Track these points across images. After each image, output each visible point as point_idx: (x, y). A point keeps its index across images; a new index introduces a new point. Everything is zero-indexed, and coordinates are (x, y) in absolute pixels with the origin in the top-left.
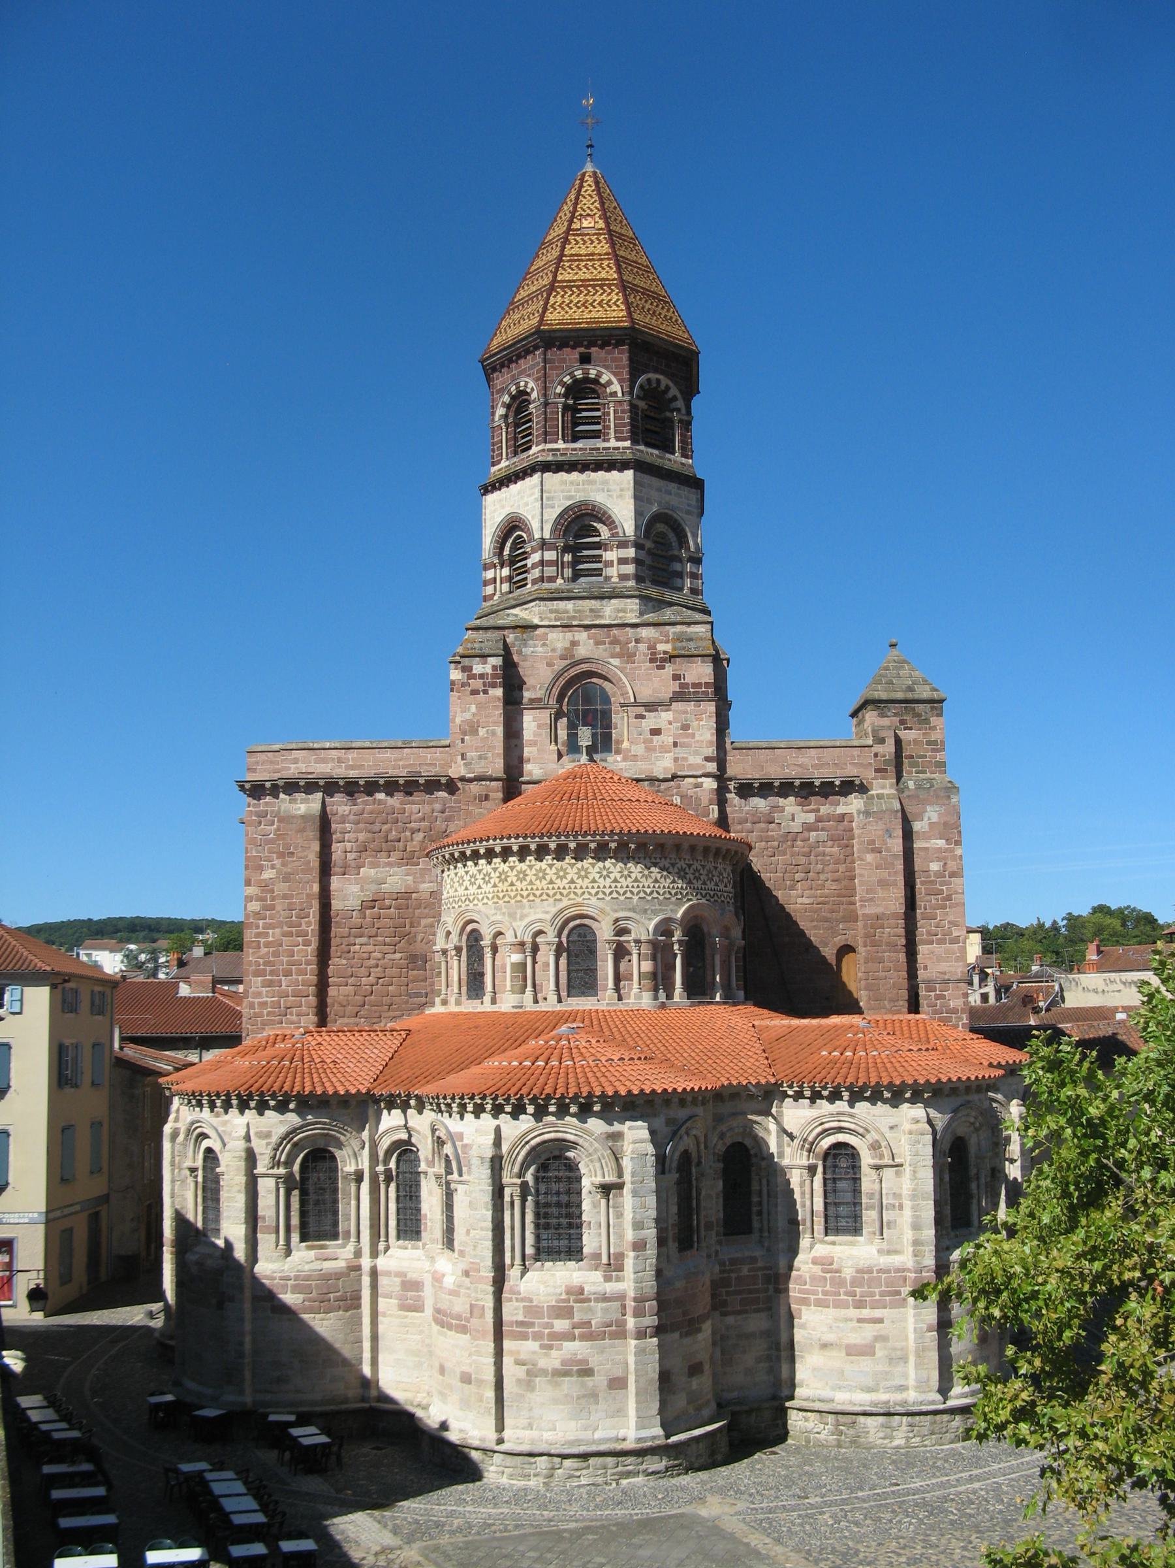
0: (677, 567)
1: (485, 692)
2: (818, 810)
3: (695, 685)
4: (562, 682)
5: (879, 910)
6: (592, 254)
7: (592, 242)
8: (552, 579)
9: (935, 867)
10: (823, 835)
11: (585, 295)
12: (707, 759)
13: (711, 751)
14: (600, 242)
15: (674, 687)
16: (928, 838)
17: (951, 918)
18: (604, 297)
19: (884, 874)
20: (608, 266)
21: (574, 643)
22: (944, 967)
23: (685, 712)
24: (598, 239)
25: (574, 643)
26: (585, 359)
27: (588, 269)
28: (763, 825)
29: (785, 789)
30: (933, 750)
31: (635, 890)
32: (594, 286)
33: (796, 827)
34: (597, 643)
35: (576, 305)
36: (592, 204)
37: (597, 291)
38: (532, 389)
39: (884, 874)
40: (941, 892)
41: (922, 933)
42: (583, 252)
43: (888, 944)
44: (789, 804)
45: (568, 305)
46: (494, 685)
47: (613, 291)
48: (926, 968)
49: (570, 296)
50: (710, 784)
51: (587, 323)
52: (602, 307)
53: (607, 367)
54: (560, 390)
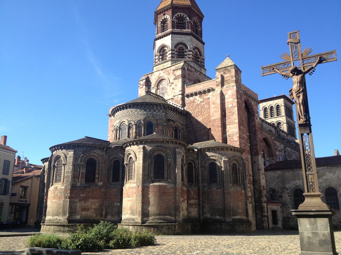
0: (185, 53)
1: (142, 87)
2: (204, 98)
3: (178, 76)
4: (157, 82)
5: (215, 118)
8: (157, 62)
9: (230, 106)
10: (204, 103)
12: (180, 91)
13: (180, 89)
15: (174, 77)
16: (228, 99)
17: (234, 118)
19: (216, 109)
21: (160, 74)
22: (232, 130)
23: (176, 82)
25: (160, 74)
26: (164, 15)
28: (192, 104)
29: (196, 94)
30: (232, 78)
31: (133, 115)
33: (199, 103)
34: (164, 73)
39: (216, 109)
40: (232, 112)
41: (227, 122)
43: (217, 126)
44: (197, 97)
46: (144, 86)
48: (228, 131)
50: (180, 96)
53: (168, 15)
54: (160, 23)
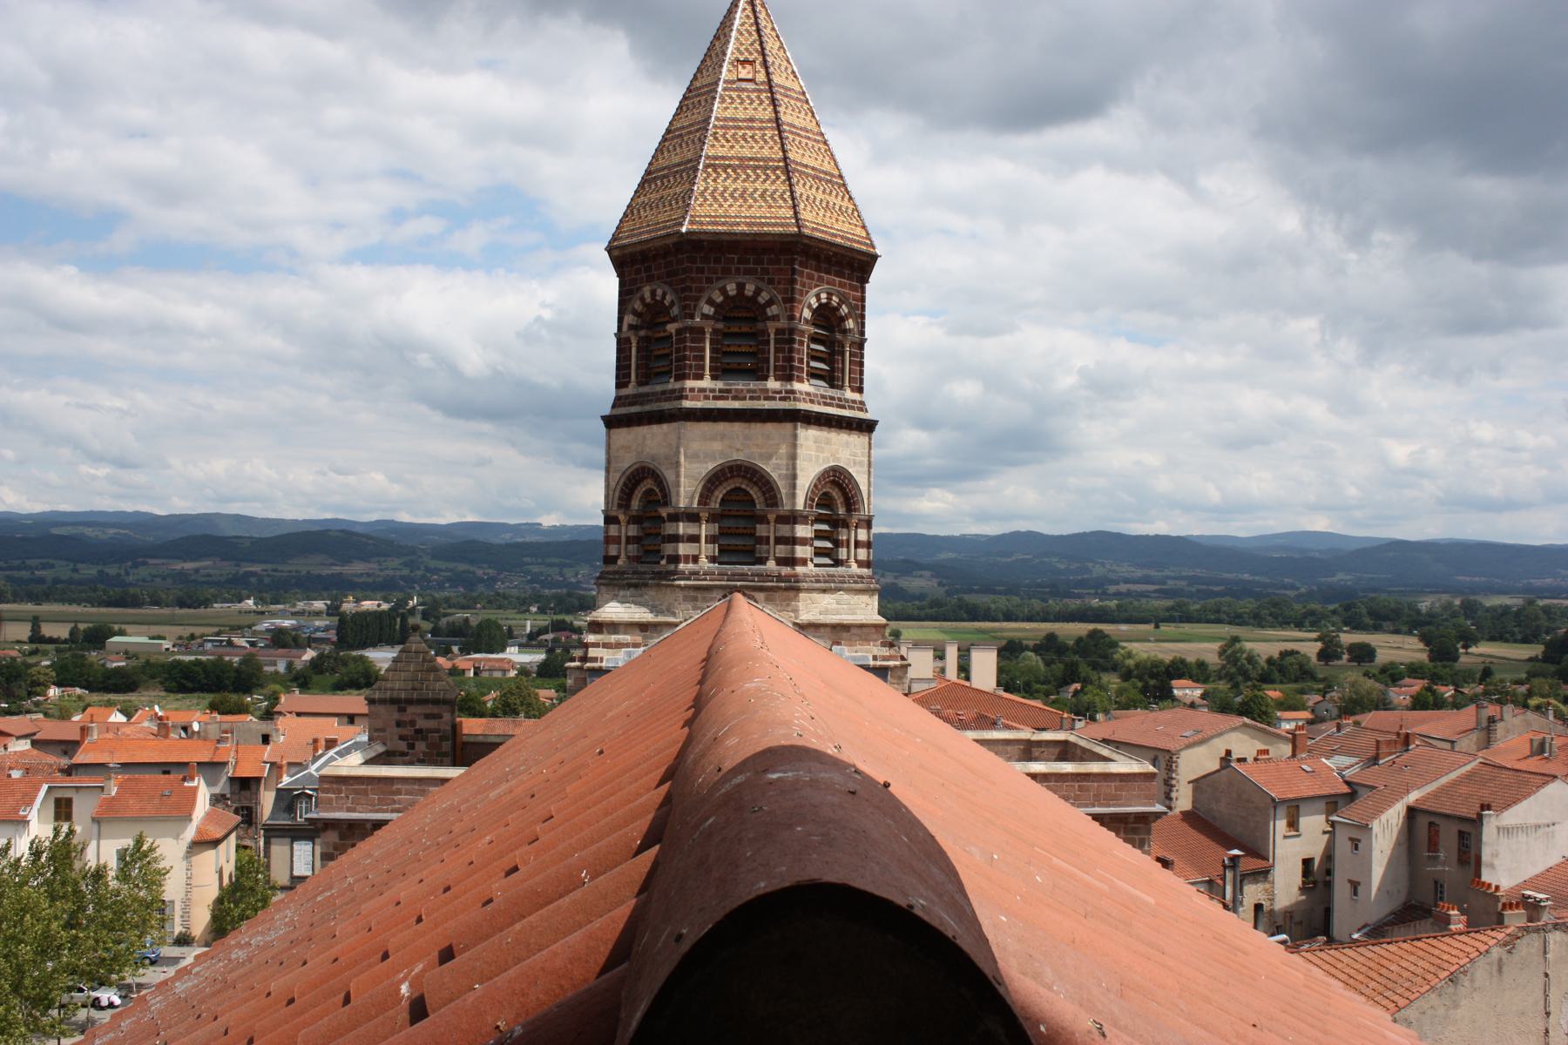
6: (752, 120)
7: (752, 102)
11: (744, 181)
14: (762, 102)
18: (767, 185)
20: (772, 138)
24: (758, 97)
27: (746, 141)
32: (755, 168)
35: (732, 195)
36: (752, 44)
37: (758, 176)
38: (672, 303)
42: (741, 115)
45: (722, 194)
47: (778, 177)
49: (725, 180)
51: (747, 224)
52: (766, 201)
